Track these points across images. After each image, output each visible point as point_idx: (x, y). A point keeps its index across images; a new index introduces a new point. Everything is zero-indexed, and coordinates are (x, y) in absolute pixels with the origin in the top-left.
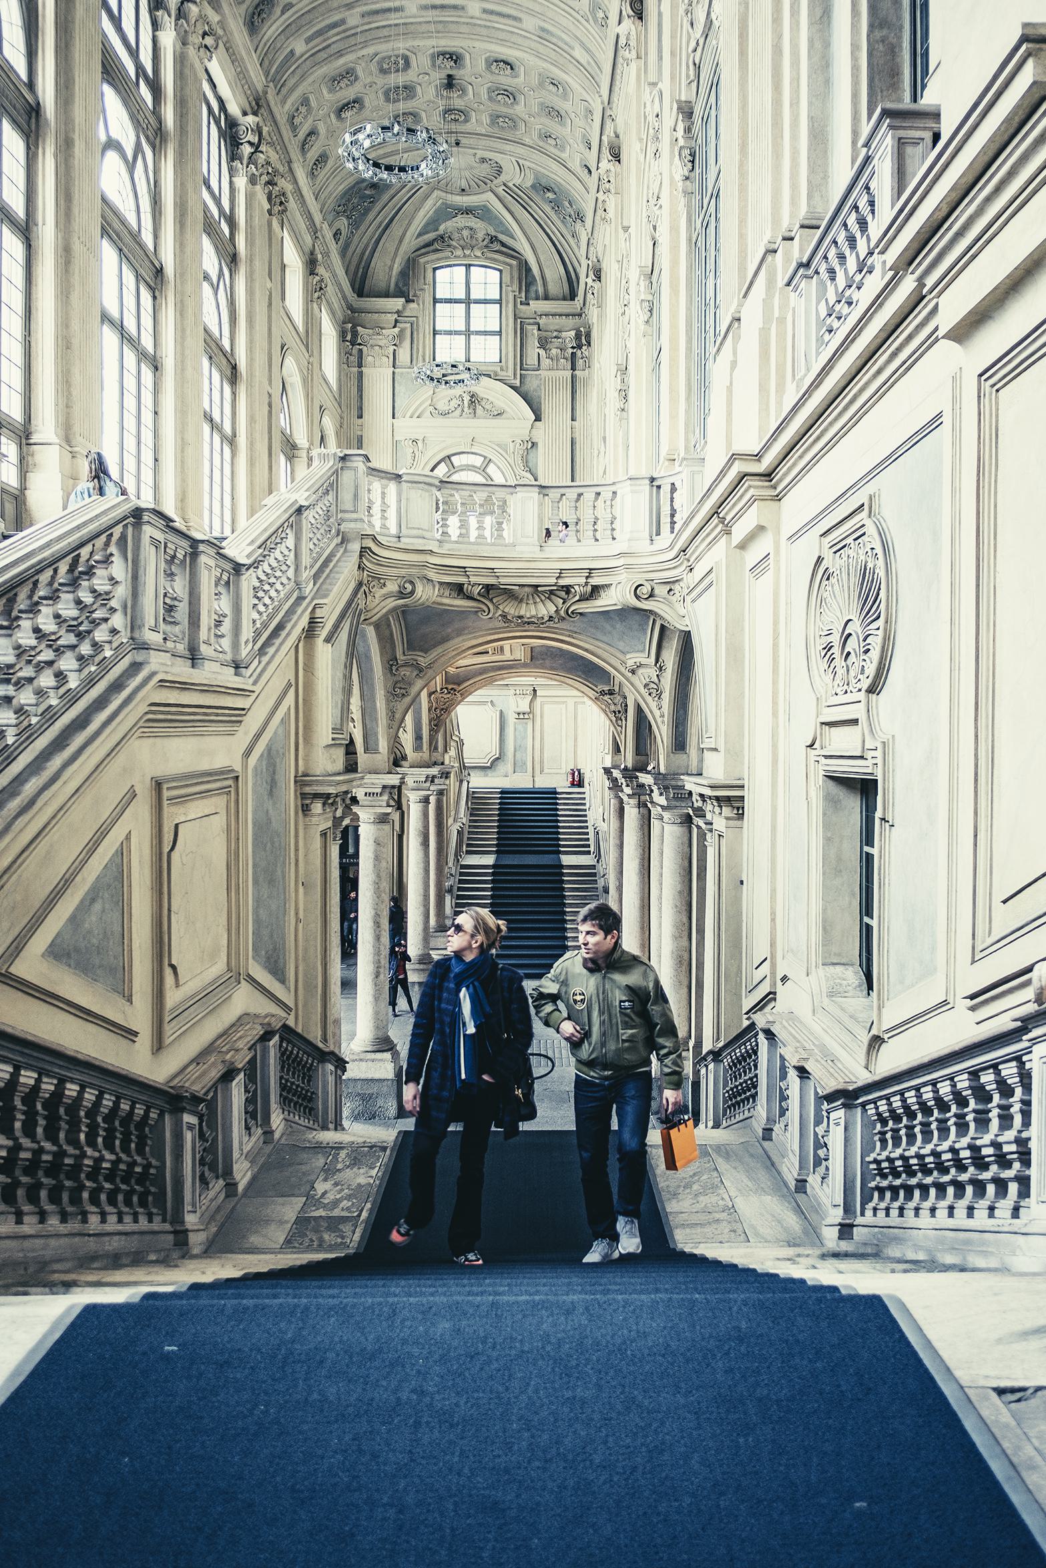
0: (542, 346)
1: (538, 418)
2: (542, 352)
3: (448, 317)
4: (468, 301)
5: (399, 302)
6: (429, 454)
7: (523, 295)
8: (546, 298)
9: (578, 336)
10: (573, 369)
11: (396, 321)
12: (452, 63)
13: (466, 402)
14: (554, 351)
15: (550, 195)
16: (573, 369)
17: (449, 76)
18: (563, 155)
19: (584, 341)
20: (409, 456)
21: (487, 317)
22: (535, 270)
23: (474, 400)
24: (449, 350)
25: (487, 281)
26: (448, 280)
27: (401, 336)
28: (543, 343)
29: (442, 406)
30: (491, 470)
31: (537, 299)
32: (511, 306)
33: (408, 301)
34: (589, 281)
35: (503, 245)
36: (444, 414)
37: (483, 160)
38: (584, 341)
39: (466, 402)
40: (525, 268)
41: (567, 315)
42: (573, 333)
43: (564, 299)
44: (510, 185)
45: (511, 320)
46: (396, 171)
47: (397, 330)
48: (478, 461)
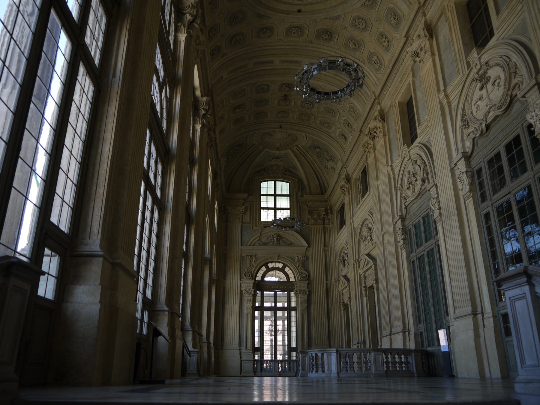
0: (310, 214)
1: (309, 246)
2: (309, 217)
3: (266, 202)
4: (275, 195)
5: (245, 195)
6: (258, 262)
7: (300, 193)
8: (311, 193)
9: (326, 210)
10: (324, 224)
11: (243, 203)
12: (288, 89)
13: (275, 239)
14: (315, 216)
15: (318, 150)
16: (324, 224)
17: (285, 95)
18: (330, 131)
19: (329, 212)
20: (248, 263)
21: (285, 202)
22: (305, 182)
23: (279, 237)
24: (266, 216)
25: (284, 187)
26: (267, 187)
27: (246, 210)
28: (311, 213)
29: (264, 240)
30: (287, 270)
31: (306, 194)
32: (295, 197)
33: (249, 195)
34: (343, 183)
35: (291, 172)
36: (265, 244)
37: (290, 135)
38: (329, 212)
39: (275, 239)
40: (301, 181)
41: (321, 201)
42: (324, 209)
43: (319, 194)
44: (300, 146)
45: (295, 203)
46: (323, 94)
47: (244, 207)
48: (280, 266)
